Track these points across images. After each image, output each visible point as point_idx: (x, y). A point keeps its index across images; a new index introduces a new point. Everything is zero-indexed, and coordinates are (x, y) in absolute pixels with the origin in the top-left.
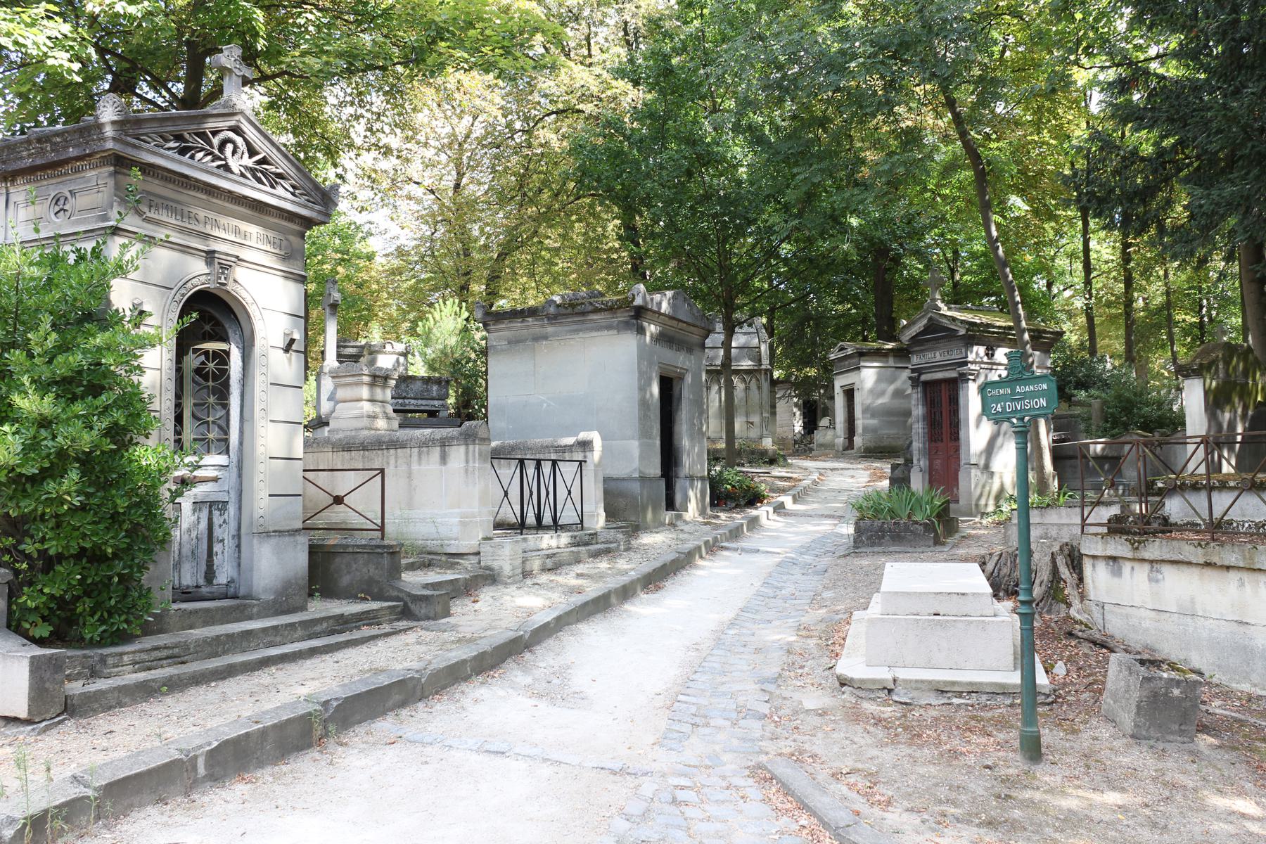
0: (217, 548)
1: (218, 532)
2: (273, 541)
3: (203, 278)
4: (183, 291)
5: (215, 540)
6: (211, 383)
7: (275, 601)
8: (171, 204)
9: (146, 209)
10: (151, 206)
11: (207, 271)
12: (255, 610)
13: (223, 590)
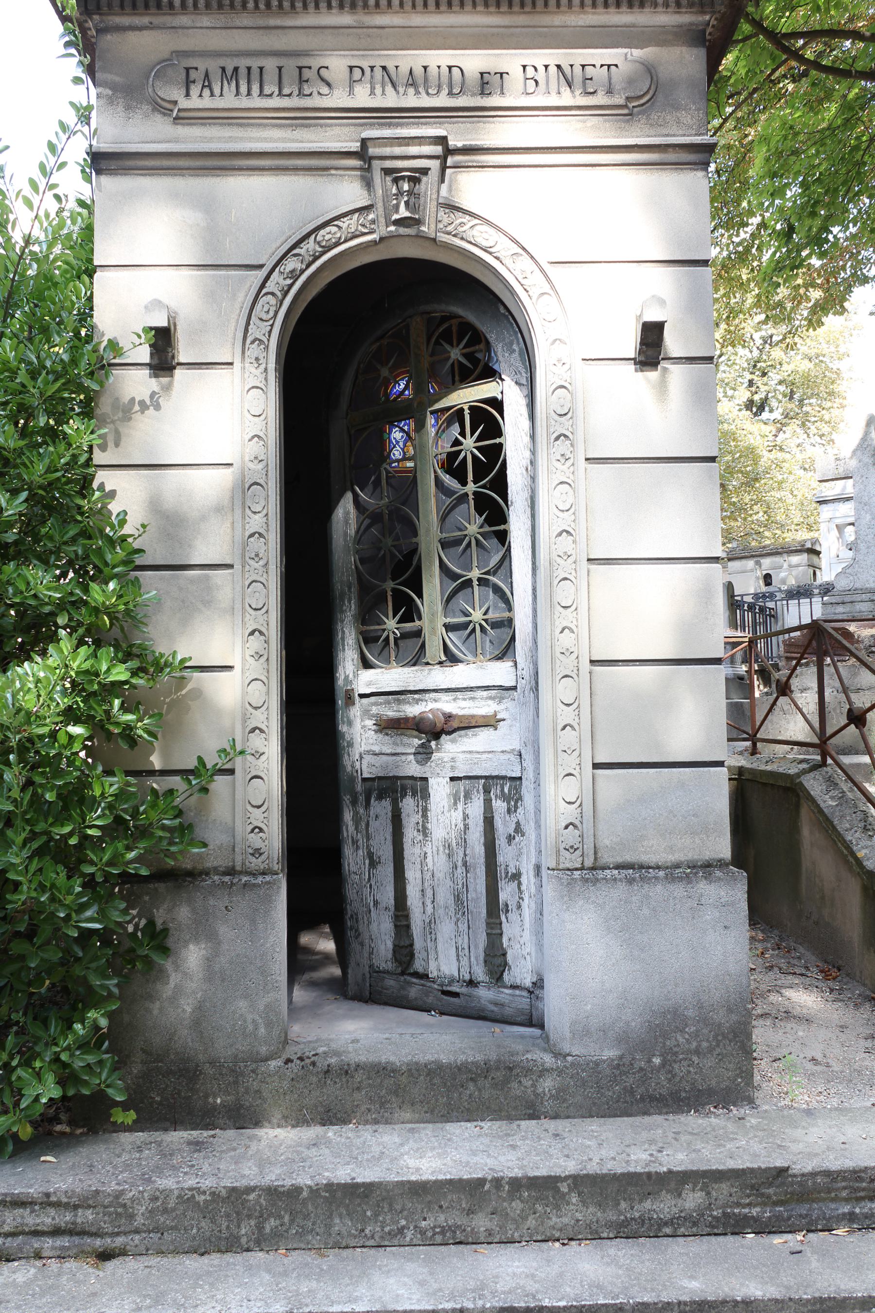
0: (506, 893)
1: (505, 855)
4: (291, 264)
5: (501, 871)
6: (471, 487)
7: (619, 1067)
8: (243, 63)
9: (176, 93)
10: (188, 83)
12: (547, 1084)
13: (522, 1001)
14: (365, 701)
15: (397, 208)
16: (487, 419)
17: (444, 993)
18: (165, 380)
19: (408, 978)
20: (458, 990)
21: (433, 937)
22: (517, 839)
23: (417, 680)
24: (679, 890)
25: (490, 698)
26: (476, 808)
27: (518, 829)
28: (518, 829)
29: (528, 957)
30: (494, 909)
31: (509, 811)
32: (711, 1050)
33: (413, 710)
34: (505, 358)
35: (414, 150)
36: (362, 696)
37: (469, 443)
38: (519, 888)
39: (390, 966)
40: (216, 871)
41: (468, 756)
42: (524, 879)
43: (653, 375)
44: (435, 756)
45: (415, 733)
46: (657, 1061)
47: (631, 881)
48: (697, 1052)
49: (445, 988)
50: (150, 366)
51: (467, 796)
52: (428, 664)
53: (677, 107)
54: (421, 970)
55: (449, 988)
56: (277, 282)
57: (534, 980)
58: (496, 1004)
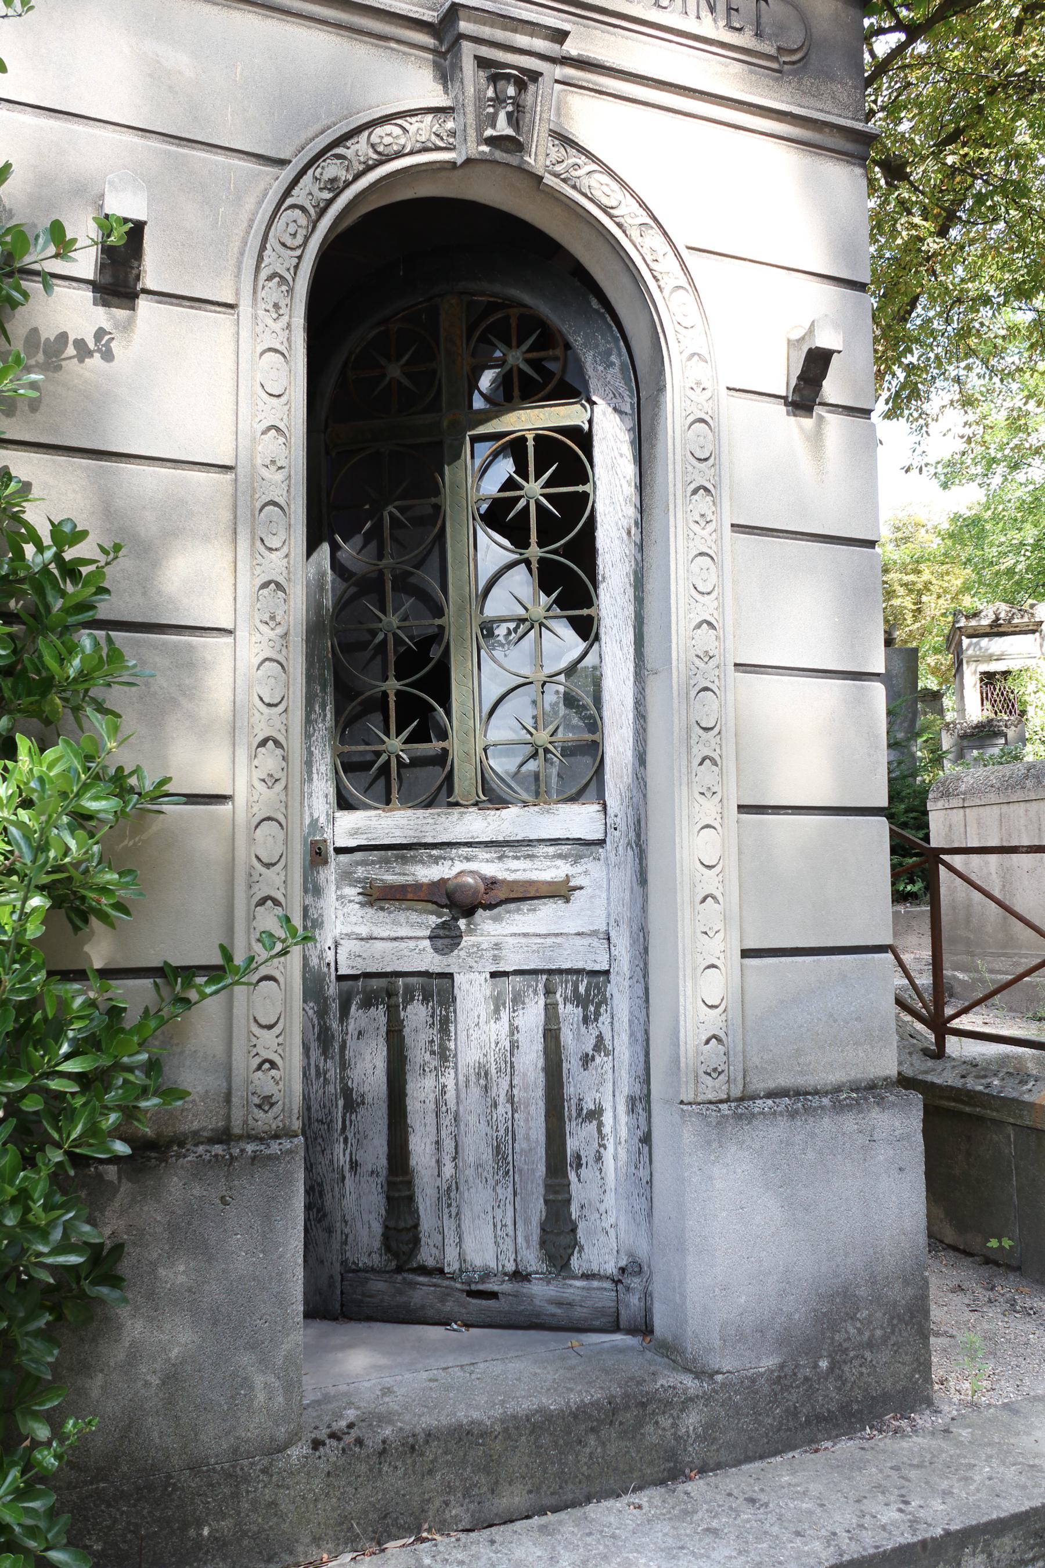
0: (578, 1139)
1: (578, 1085)
2: (772, 1134)
3: (423, 128)
5: (570, 1109)
7: (780, 1379)
11: (441, 100)
12: (692, 1420)
13: (603, 1296)
14: (343, 858)
15: (493, 122)
16: (567, 457)
17: (471, 1294)
18: (121, 314)
19: (410, 1276)
20: (496, 1288)
21: (454, 1210)
22: (598, 1060)
23: (439, 828)
24: (849, 1122)
25: (560, 856)
26: (532, 1016)
27: (599, 1045)
28: (599, 1045)
29: (612, 1232)
30: (558, 1163)
31: (586, 1020)
32: (885, 1339)
33: (427, 873)
34: (601, 374)
35: (522, 40)
36: (339, 851)
37: (534, 489)
38: (600, 1132)
39: (376, 1260)
40: (197, 1137)
41: (523, 940)
42: (607, 1118)
43: (808, 423)
44: (467, 941)
45: (431, 907)
46: (824, 1364)
47: (793, 1114)
48: (870, 1345)
49: (473, 1287)
50: (95, 286)
51: (518, 1000)
52: (457, 804)
53: (831, 78)
54: (430, 1263)
55: (481, 1287)
56: (306, 192)
57: (623, 1263)
58: (559, 1304)
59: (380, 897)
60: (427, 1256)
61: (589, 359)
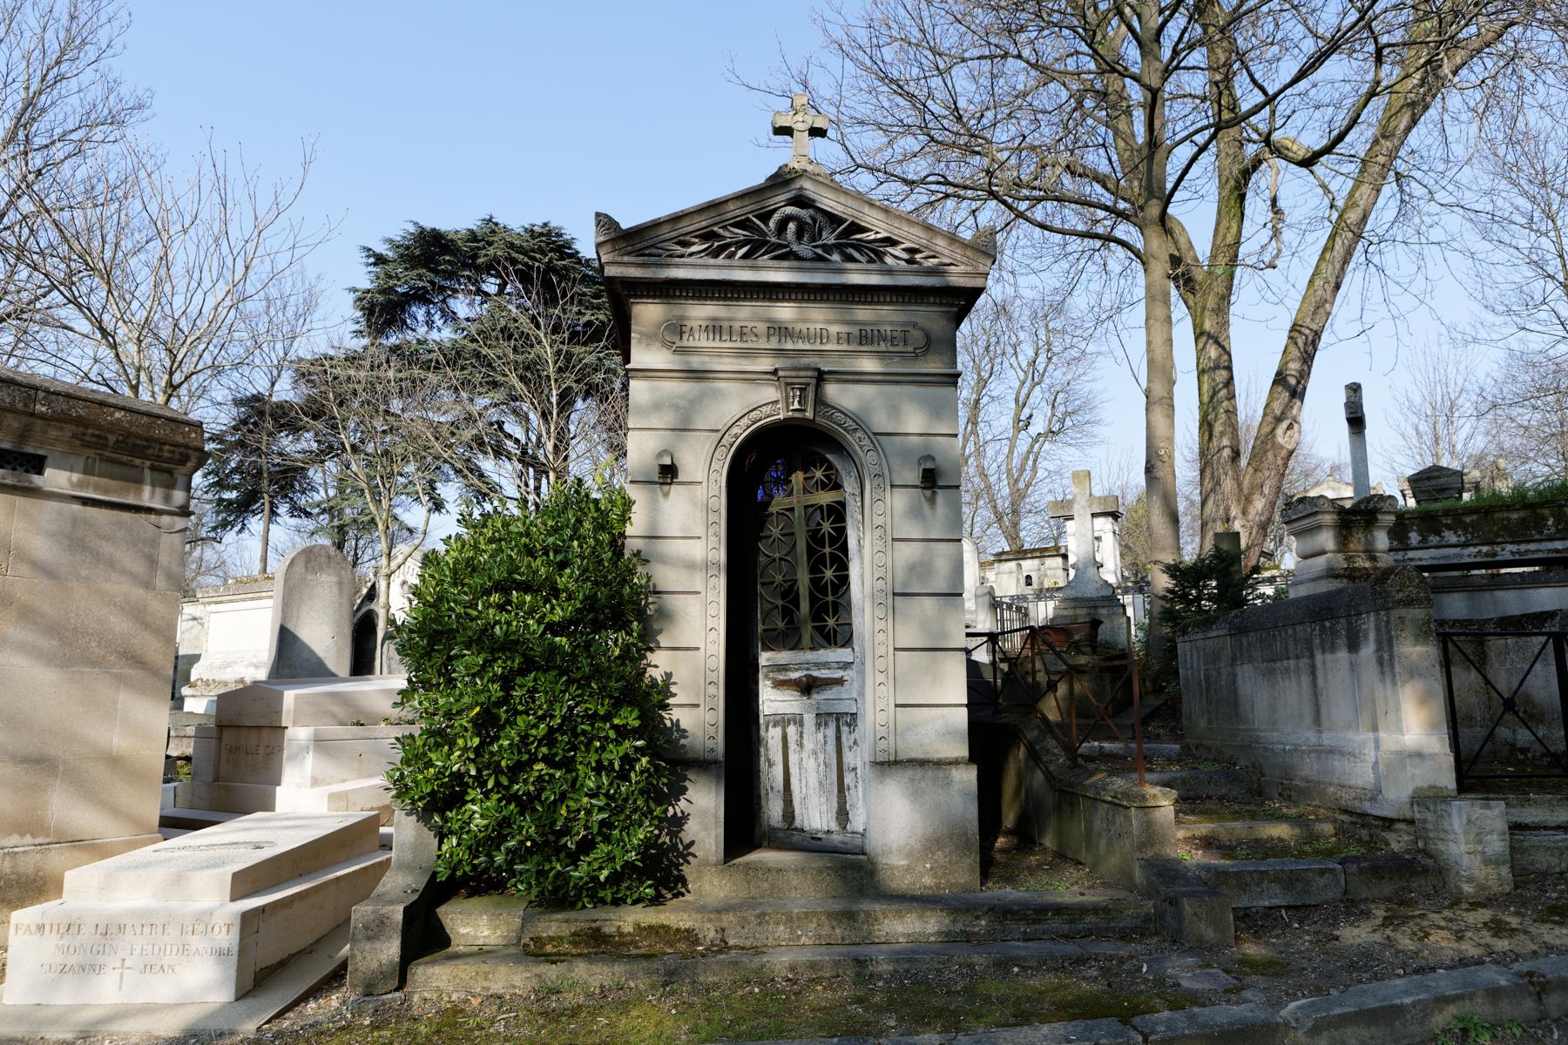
0: (849, 779)
5: (845, 767)
27: (855, 742)
28: (855, 742)
30: (842, 789)
39: (780, 825)
43: (928, 493)
56: (727, 440)
59: (779, 684)
60: (797, 823)
61: (843, 473)
